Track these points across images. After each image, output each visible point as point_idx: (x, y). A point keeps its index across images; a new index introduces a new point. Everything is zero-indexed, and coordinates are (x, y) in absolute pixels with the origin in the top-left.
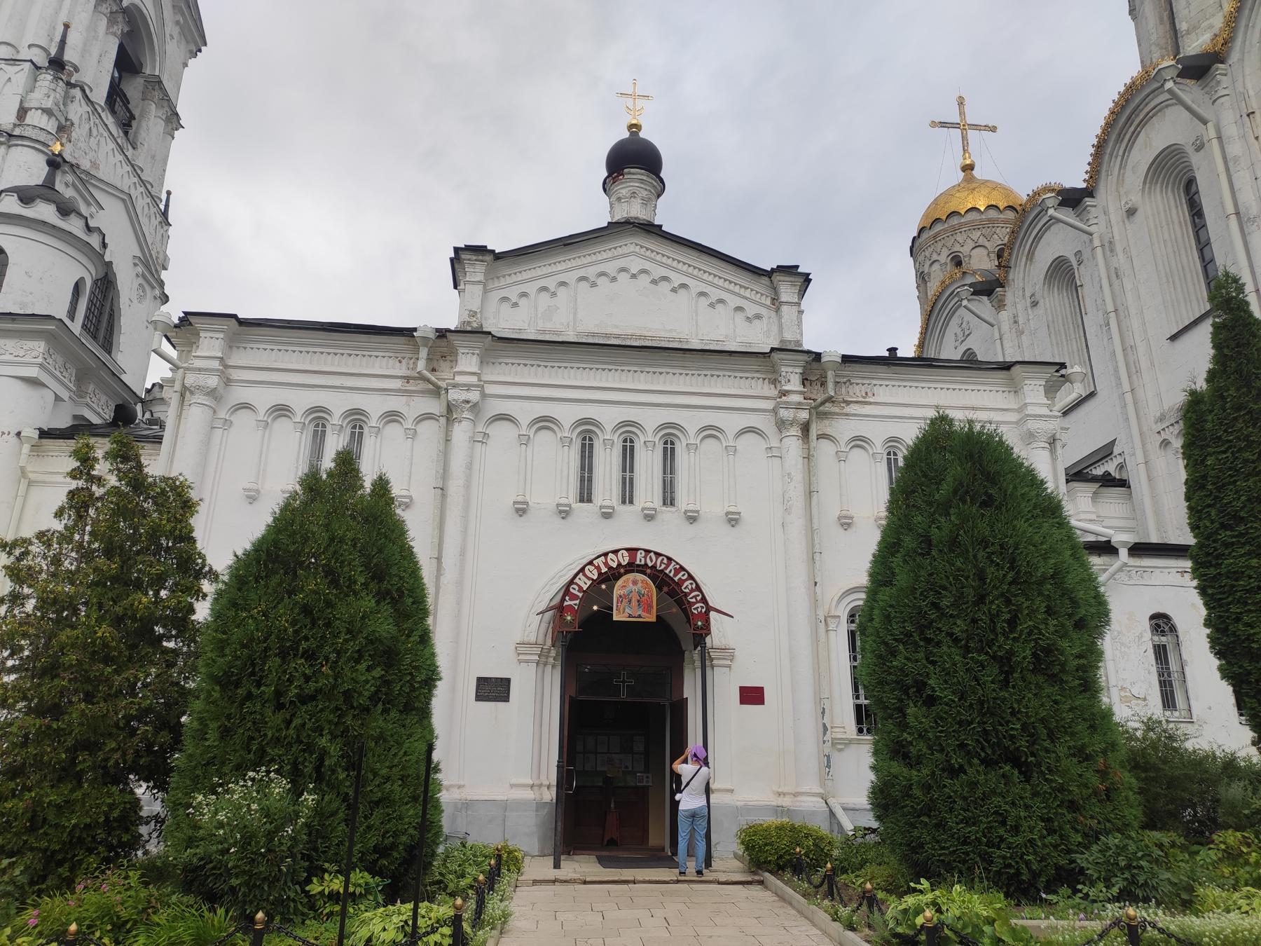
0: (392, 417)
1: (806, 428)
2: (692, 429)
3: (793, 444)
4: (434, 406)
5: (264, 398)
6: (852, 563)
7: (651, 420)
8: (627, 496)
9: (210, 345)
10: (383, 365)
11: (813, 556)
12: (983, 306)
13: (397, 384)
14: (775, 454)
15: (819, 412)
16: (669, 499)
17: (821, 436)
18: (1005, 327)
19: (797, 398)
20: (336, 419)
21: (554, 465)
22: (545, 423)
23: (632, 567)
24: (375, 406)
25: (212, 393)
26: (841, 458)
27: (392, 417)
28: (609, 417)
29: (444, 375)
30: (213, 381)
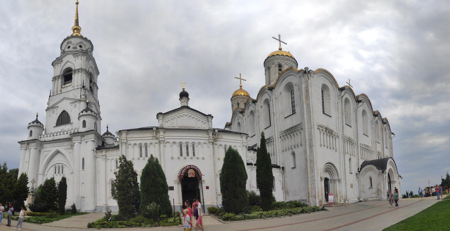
0: (151, 143)
1: (213, 143)
2: (197, 143)
3: (211, 146)
4: (157, 141)
5: (132, 143)
7: (190, 141)
9: (124, 135)
10: (148, 135)
13: (151, 138)
15: (215, 140)
19: (211, 138)
20: (143, 145)
21: (176, 149)
22: (174, 143)
24: (148, 142)
25: (126, 143)
27: (151, 143)
28: (184, 141)
29: (158, 136)
30: (125, 141)
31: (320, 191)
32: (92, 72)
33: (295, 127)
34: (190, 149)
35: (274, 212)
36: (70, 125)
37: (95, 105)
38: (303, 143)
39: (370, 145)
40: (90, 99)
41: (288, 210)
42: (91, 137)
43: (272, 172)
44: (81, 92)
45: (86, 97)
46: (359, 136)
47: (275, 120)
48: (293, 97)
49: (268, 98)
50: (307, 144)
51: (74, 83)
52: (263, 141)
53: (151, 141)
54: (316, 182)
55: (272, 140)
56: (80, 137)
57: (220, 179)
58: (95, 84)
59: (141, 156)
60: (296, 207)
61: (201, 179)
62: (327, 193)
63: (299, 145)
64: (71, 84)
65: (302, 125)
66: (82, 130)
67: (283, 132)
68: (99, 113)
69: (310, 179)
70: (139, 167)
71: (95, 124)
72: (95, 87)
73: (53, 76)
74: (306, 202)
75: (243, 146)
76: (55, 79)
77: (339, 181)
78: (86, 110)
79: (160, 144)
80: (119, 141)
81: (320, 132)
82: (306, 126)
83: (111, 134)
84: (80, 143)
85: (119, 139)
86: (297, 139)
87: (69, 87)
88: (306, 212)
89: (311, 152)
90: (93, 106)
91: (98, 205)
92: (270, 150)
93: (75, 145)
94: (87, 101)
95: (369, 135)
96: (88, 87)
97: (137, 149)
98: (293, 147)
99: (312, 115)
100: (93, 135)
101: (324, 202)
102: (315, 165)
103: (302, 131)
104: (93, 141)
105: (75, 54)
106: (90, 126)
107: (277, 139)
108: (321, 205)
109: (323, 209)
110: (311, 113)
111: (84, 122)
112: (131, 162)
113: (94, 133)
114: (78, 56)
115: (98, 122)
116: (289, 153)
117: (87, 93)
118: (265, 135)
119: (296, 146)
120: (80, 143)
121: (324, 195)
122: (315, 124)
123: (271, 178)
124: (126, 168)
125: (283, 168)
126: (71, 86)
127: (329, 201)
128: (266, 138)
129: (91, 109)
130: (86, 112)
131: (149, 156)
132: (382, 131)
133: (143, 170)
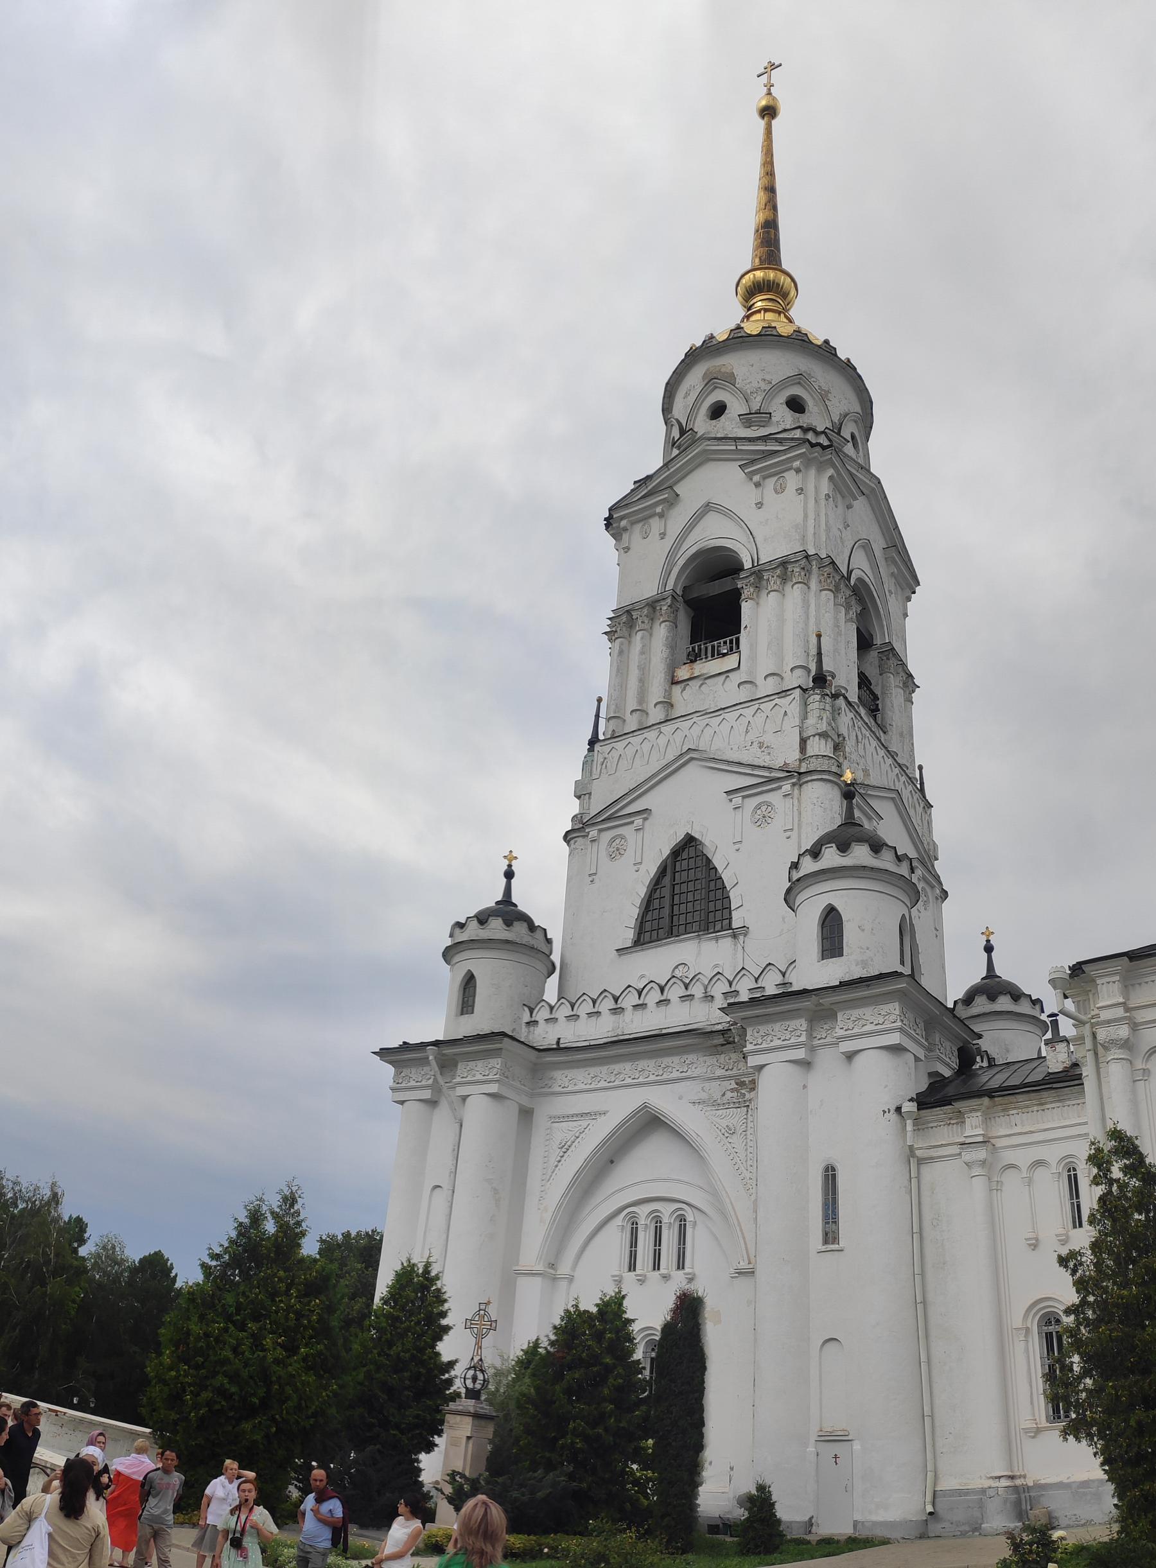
36: (726, 943)
37: (897, 799)
42: (883, 1021)
44: (804, 716)
45: (837, 747)
51: (753, 658)
56: (801, 1024)
58: (892, 658)
64: (731, 661)
68: (927, 857)
71: (905, 929)
72: (894, 681)
73: (609, 605)
76: (625, 622)
78: (844, 836)
87: (719, 681)
90: (885, 808)
91: (938, 1489)
94: (848, 776)
96: (846, 676)
100: (894, 1008)
105: (761, 459)
106: (869, 947)
111: (831, 921)
113: (901, 996)
115: (921, 918)
117: (846, 719)
126: (736, 678)
129: (876, 838)
130: (843, 848)
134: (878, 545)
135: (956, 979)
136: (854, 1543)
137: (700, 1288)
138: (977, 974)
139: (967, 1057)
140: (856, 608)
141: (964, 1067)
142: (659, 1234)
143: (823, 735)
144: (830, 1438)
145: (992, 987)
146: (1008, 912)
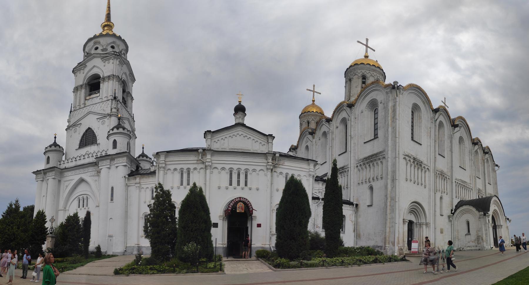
0: (195, 169)
3: (269, 173)
4: (203, 166)
5: (172, 167)
6: (278, 198)
8: (239, 184)
9: (162, 158)
10: (192, 158)
11: (271, 197)
12: (310, 137)
13: (195, 162)
14: (266, 175)
16: (246, 185)
17: (275, 172)
18: (314, 143)
20: (185, 170)
21: (225, 177)
22: (223, 169)
23: (240, 201)
24: (192, 167)
25: (164, 168)
26: (278, 176)
27: (195, 169)
30: (164, 165)
31: (401, 236)
32: (126, 79)
33: (376, 155)
34: (242, 177)
35: (340, 259)
36: (96, 146)
38: (384, 176)
39: (467, 180)
40: (123, 113)
41: (357, 258)
42: (123, 160)
43: (342, 209)
44: (112, 104)
45: (117, 110)
46: (454, 169)
47: (352, 145)
48: (376, 117)
49: (347, 116)
50: (389, 177)
51: (102, 94)
52: (335, 170)
53: (195, 166)
54: (397, 225)
55: (346, 170)
56: (109, 161)
57: (277, 215)
58: (129, 94)
59: (182, 184)
60: (369, 255)
61: (251, 213)
62: (410, 239)
63: (379, 177)
64: (98, 95)
65: (384, 153)
66: (112, 152)
67: (360, 160)
68: (133, 131)
69: (388, 221)
70: (178, 198)
71: (128, 144)
72: (129, 98)
74: (381, 249)
75: (310, 175)
77: (427, 224)
78: (118, 127)
79: (206, 169)
80: (156, 166)
81: (407, 163)
82: (390, 154)
83: (147, 157)
84: (109, 168)
85: (157, 163)
86: (377, 170)
87: (96, 98)
88: (380, 262)
89: (394, 187)
91: (128, 245)
92: (343, 181)
93: (102, 171)
94: (119, 116)
95: (467, 167)
96: (120, 97)
97: (177, 176)
98: (371, 180)
99: (397, 141)
100: (125, 158)
101: (406, 251)
102: (397, 203)
103: (384, 161)
104: (125, 166)
105: (105, 57)
106: (122, 147)
107: (352, 168)
108: (400, 254)
109: (403, 259)
110: (397, 139)
111: (115, 142)
112: (168, 191)
113: (127, 156)
114: (109, 60)
115: (131, 142)
116: (366, 186)
117: (119, 105)
118: (338, 164)
119: (375, 178)
120: (109, 168)
121: (407, 242)
122: (401, 153)
123: (341, 218)
124: (162, 198)
125: (357, 205)
127: (412, 250)
128: (338, 167)
129: (124, 127)
130: (118, 129)
131: (191, 184)
132: (483, 163)
133: (183, 201)
134: (128, 73)
135: (137, 154)
136: (113, 256)
137: (90, 210)
138: (141, 153)
139: (138, 167)
140: (122, 85)
141: (137, 170)
142: (83, 201)
143: (115, 108)
144: (110, 236)
145: (143, 155)
146: (147, 141)
